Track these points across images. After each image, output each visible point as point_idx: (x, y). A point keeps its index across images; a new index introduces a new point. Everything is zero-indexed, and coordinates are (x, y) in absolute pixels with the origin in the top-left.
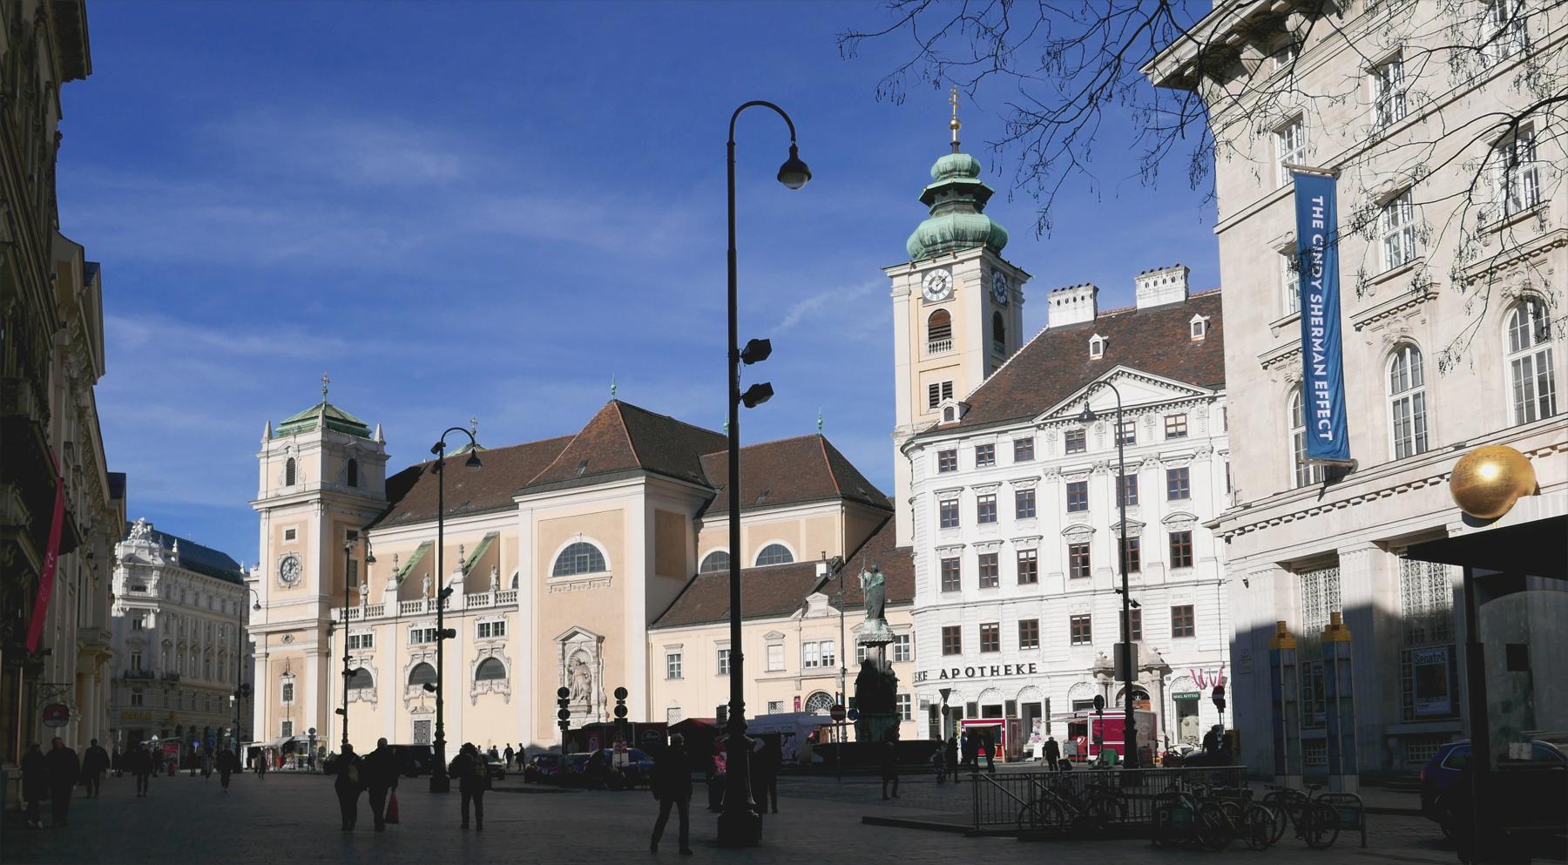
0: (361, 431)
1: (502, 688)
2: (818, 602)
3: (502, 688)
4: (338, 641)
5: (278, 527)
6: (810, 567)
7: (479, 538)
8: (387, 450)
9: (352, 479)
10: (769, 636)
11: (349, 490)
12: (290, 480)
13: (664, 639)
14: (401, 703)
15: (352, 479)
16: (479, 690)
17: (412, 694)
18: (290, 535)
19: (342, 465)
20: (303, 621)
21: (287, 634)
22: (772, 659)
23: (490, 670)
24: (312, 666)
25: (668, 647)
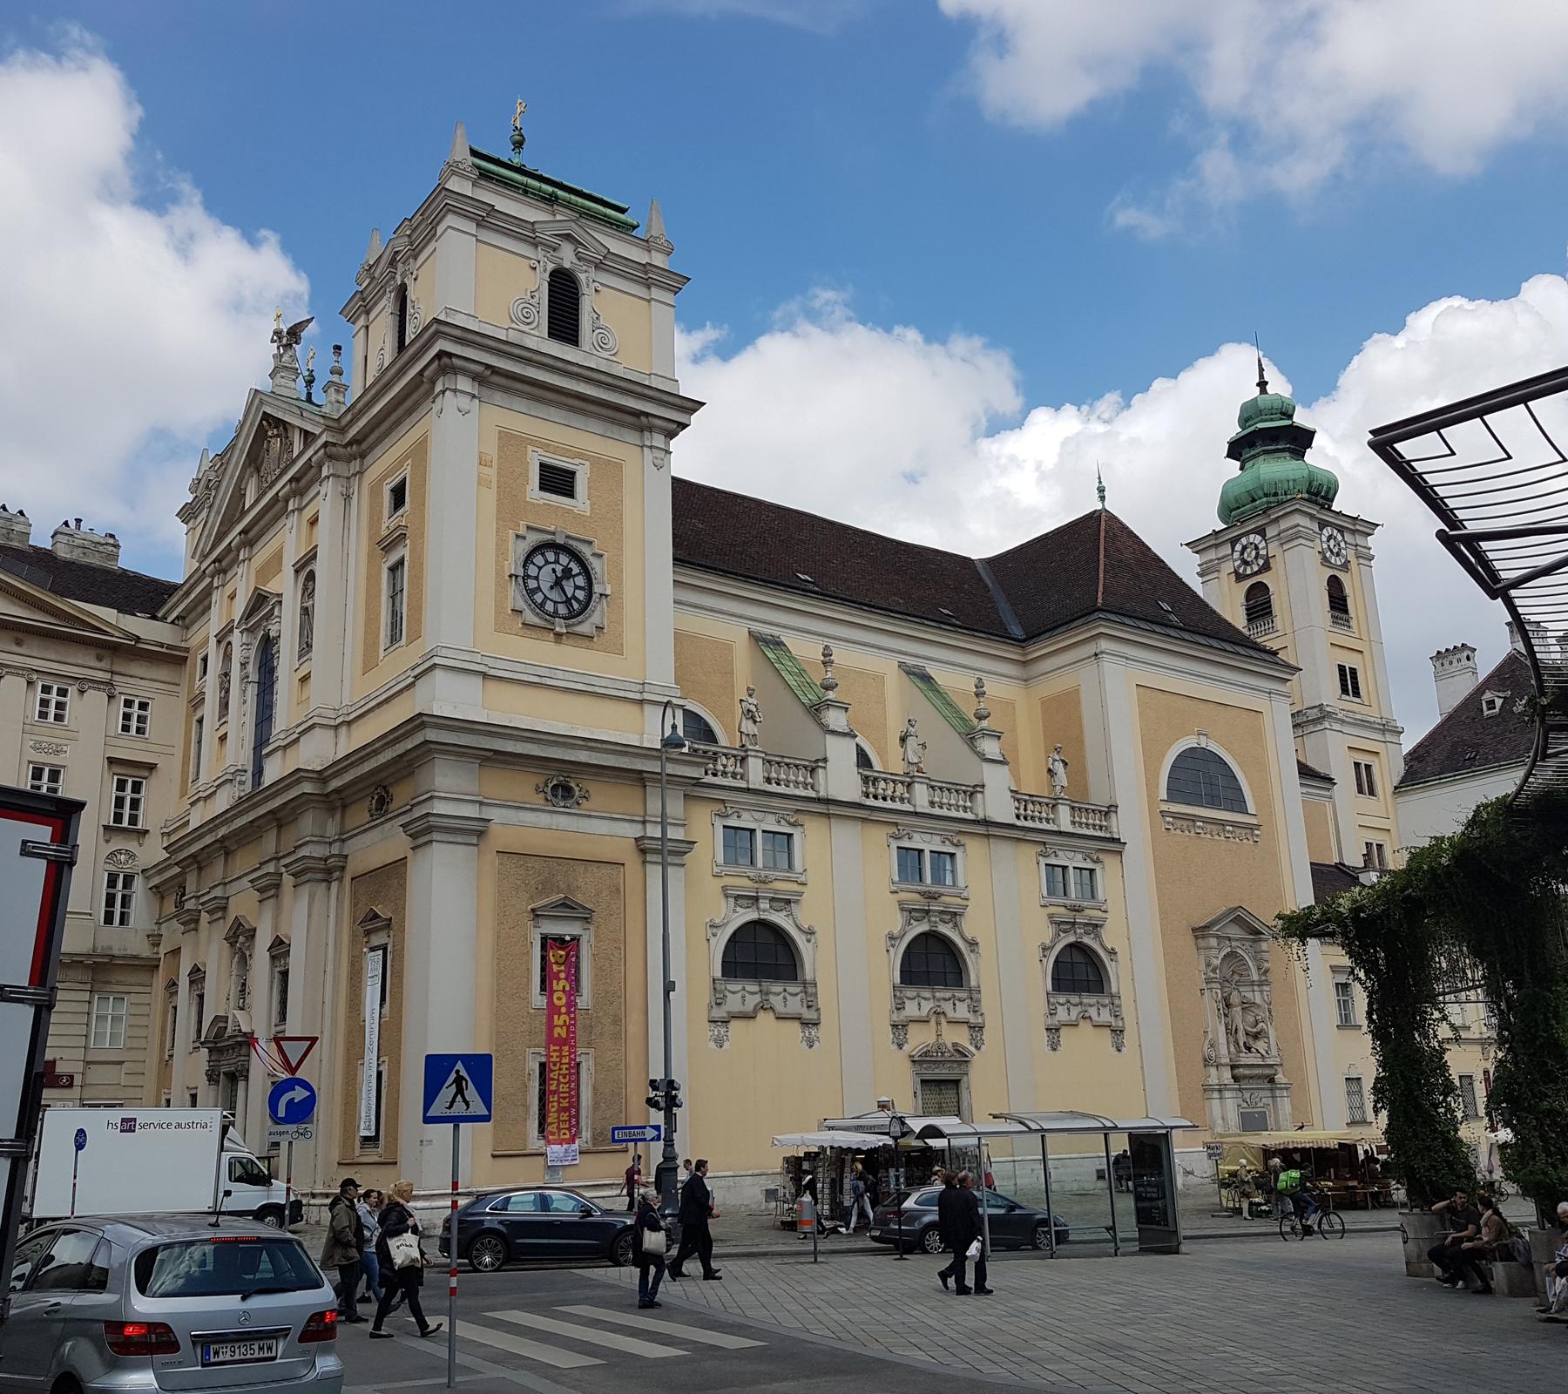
3: (1106, 1016)
16: (1062, 1014)
17: (911, 1009)
18: (557, 481)
23: (1079, 971)
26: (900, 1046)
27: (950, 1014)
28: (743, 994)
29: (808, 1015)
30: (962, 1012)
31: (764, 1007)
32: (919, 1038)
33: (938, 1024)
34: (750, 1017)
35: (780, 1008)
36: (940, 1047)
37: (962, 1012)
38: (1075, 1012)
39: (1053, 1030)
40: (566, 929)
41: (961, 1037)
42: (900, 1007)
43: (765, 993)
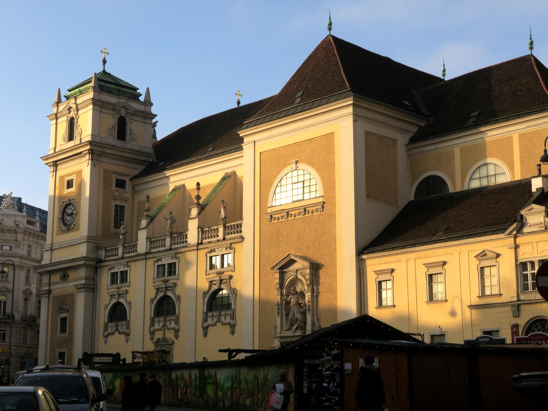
0: (131, 92)
1: (228, 320)
2: (535, 216)
3: (228, 320)
4: (105, 278)
5: (62, 178)
6: (526, 184)
7: (216, 178)
8: (154, 110)
9: (122, 134)
10: (482, 255)
11: (119, 143)
12: (71, 137)
13: (375, 263)
14: (148, 335)
15: (122, 131)
16: (210, 321)
17: (157, 326)
18: (70, 184)
19: (111, 121)
20: (74, 260)
21: (64, 271)
22: (487, 282)
24: (81, 300)
25: (378, 273)
26: (152, 339)
27: (169, 326)
28: (112, 327)
29: (127, 331)
30: (173, 325)
31: (117, 330)
32: (159, 335)
33: (164, 330)
34: (113, 334)
35: (121, 330)
36: (164, 339)
37: (173, 325)
38: (215, 319)
39: (205, 329)
40: (64, 315)
41: (170, 335)
42: (152, 325)
43: (117, 325)
